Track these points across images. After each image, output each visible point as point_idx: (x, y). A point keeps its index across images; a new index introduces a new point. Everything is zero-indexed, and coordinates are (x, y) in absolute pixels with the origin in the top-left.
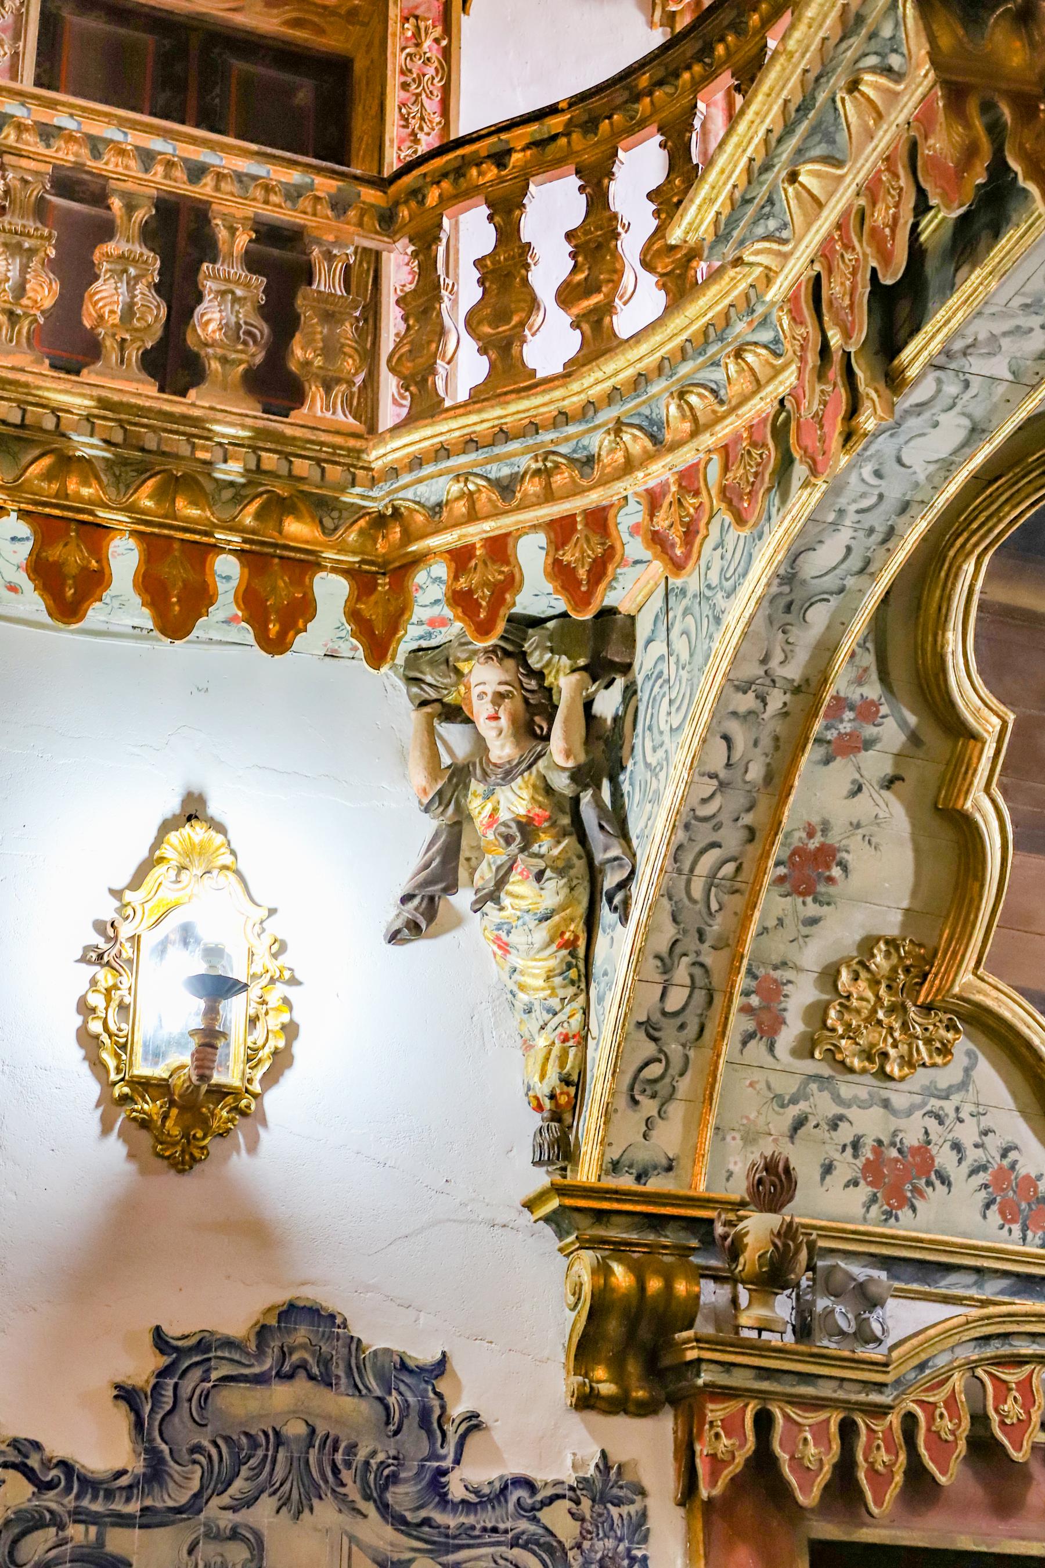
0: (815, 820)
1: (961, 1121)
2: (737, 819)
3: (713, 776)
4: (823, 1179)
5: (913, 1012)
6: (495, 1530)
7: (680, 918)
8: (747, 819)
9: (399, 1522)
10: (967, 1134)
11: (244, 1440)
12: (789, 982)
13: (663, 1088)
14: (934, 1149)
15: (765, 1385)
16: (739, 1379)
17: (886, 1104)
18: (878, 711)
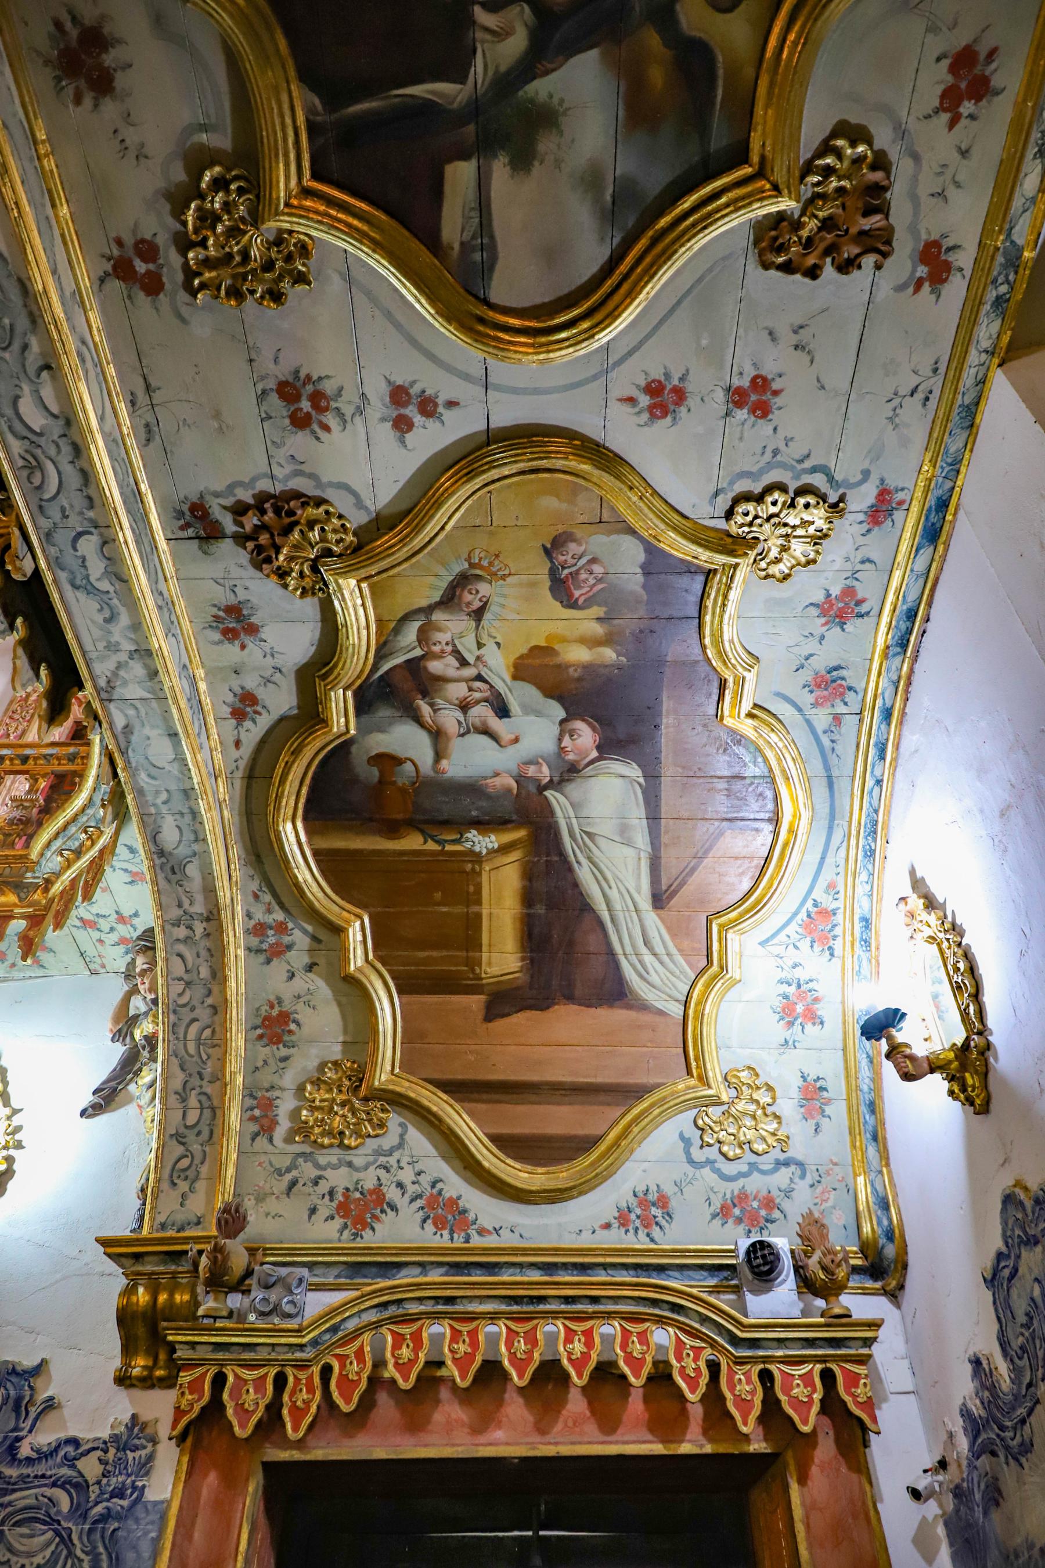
0: (272, 998)
1: (402, 1168)
2: (203, 1002)
3: (180, 979)
4: (310, 1217)
5: (357, 1103)
7: (185, 1067)
8: (209, 1001)
10: (407, 1176)
13: (191, 1173)
14: (385, 1189)
15: (220, 1356)
16: (201, 1353)
17: (350, 1164)
18: (287, 927)
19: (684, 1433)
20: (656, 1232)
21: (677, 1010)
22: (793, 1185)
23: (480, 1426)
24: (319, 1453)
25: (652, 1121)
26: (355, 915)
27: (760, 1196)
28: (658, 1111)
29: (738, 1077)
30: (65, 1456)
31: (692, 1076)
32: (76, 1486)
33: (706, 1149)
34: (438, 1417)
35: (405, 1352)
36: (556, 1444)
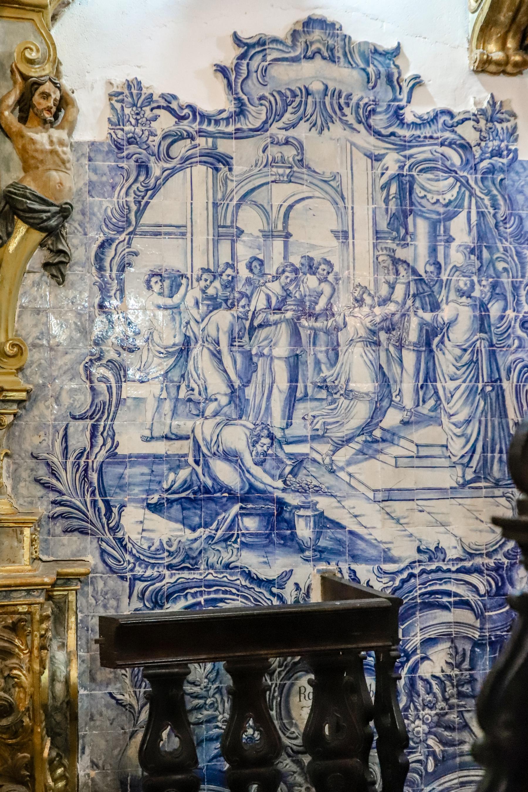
6: (431, 137)
11: (288, 93)
30: (444, 123)
32: (462, 146)
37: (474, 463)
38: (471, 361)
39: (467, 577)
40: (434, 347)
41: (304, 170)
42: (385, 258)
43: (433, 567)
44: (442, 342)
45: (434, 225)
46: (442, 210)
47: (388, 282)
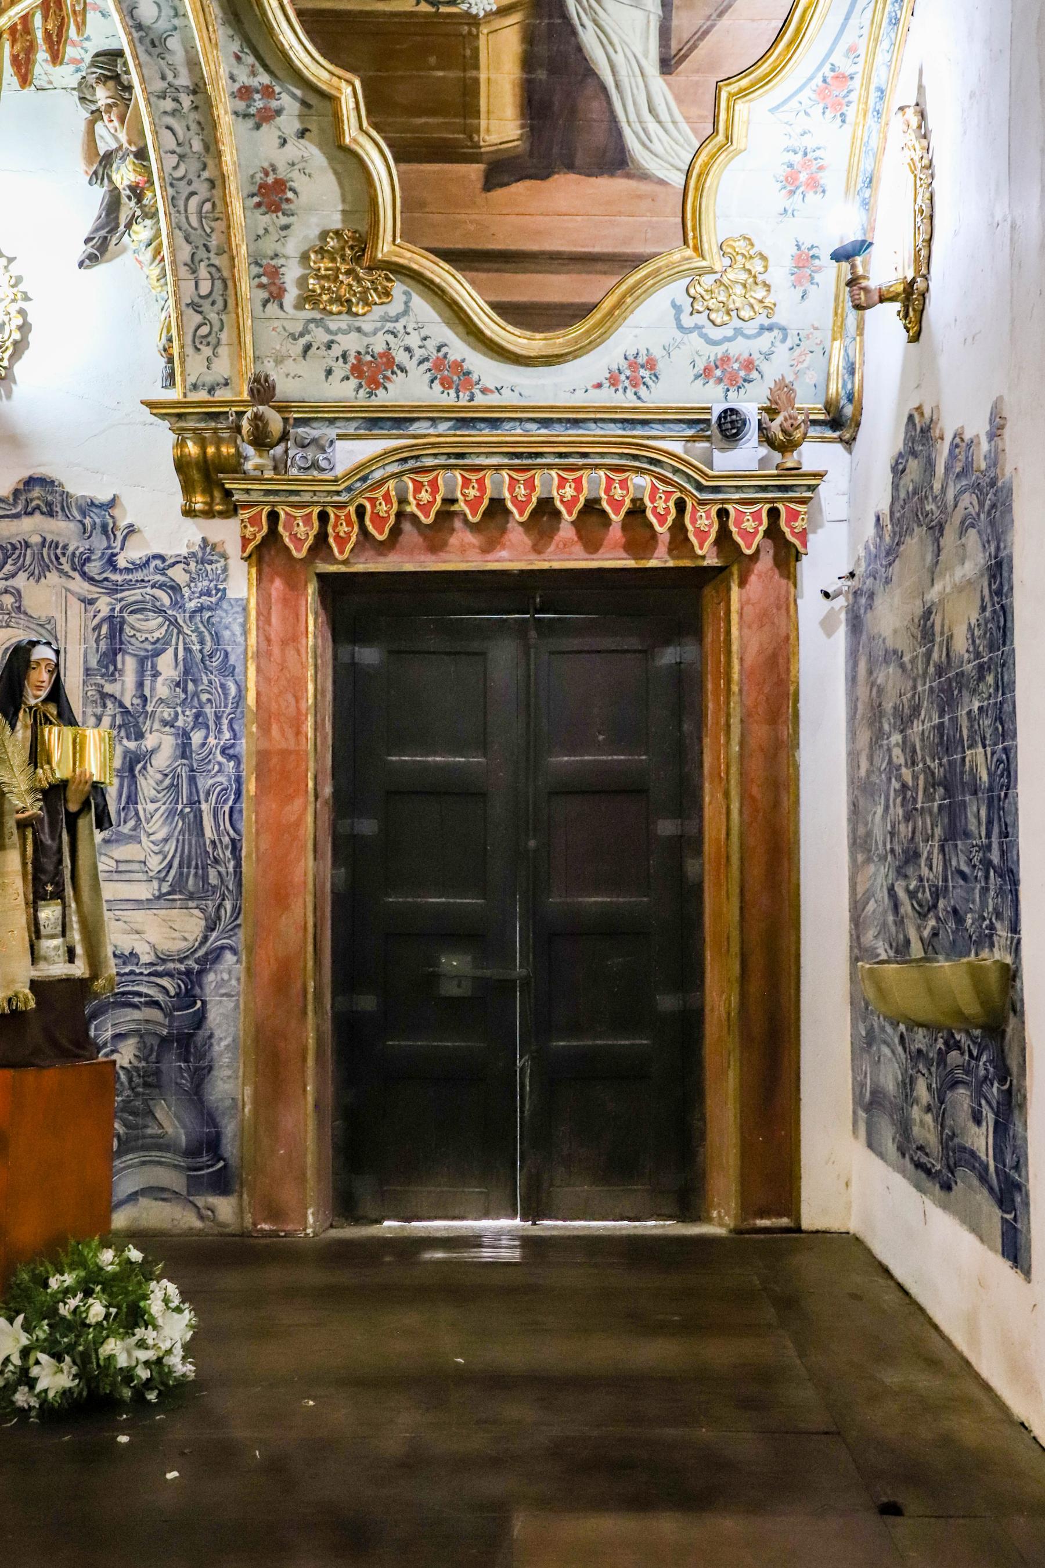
1: (408, 334)
4: (327, 378)
5: (361, 272)
6: (143, 581)
9: (91, 580)
10: (414, 341)
11: (9, 546)
12: (283, 266)
13: (212, 339)
14: (393, 353)
15: (271, 498)
16: (254, 497)
17: (359, 330)
19: (653, 552)
20: (643, 391)
21: (677, 180)
22: (773, 349)
23: (488, 548)
24: (359, 568)
25: (645, 292)
26: (346, 80)
27: (741, 359)
28: (652, 282)
29: (734, 248)
31: (688, 246)
33: (696, 315)
34: (453, 540)
35: (425, 496)
36: (549, 560)
37: (170, 878)
38: (172, 785)
39: (159, 981)
40: (137, 772)
41: (22, 616)
42: (94, 693)
43: (127, 970)
44: (144, 768)
45: (142, 661)
46: (150, 647)
47: (95, 715)
